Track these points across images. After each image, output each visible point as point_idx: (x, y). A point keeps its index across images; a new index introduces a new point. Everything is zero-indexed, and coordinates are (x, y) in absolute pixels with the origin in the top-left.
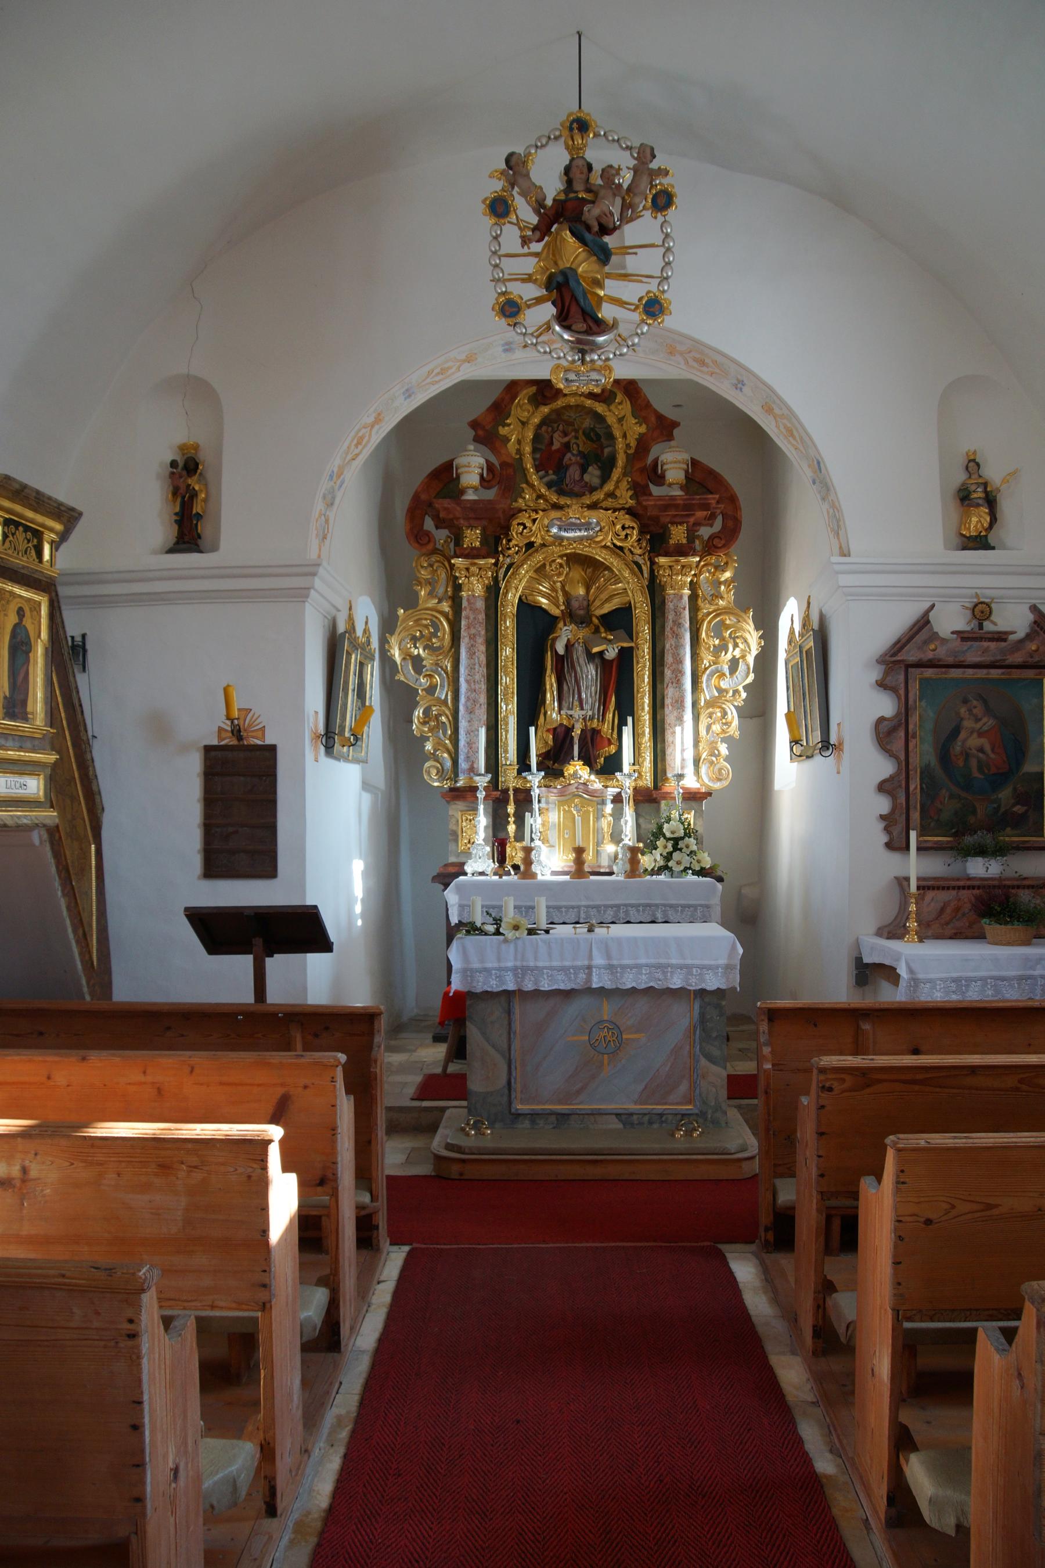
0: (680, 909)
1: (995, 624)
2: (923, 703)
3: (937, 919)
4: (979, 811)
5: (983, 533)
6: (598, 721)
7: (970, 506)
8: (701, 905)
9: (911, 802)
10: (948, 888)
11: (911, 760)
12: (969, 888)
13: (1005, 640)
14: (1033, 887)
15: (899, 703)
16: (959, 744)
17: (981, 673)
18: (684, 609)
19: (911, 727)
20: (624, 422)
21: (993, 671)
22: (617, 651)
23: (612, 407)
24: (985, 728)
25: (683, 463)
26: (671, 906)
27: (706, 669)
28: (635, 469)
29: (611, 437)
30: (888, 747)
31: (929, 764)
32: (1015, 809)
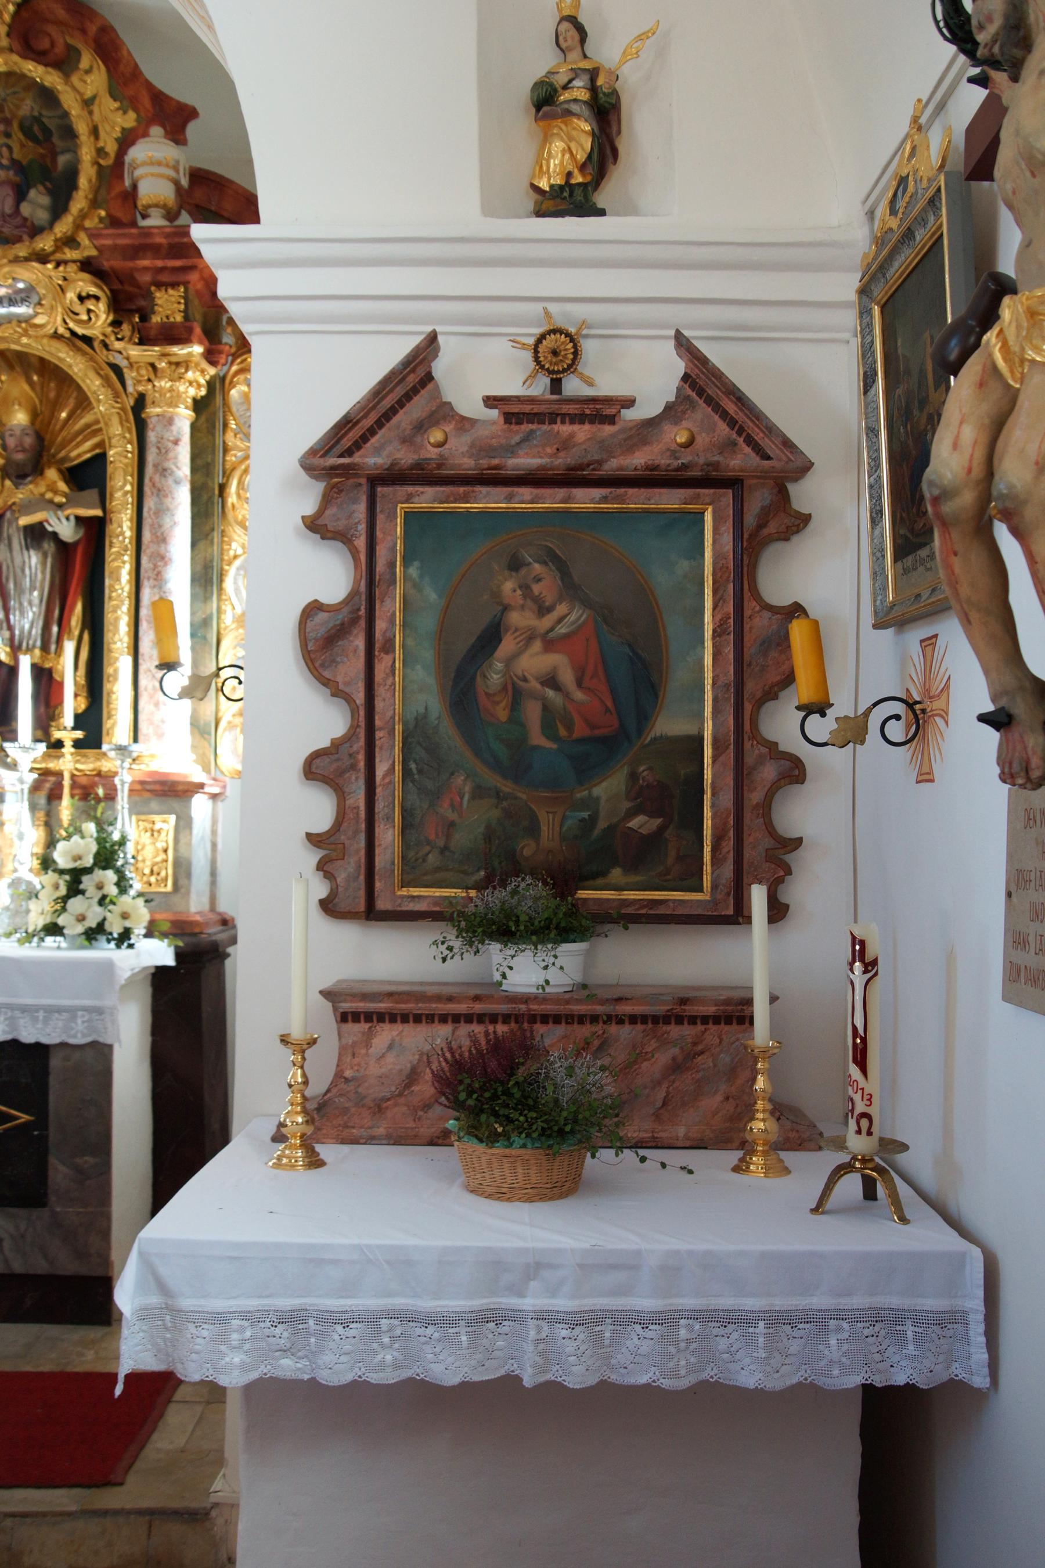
0: (41, 1015)
1: (590, 383)
2: (414, 571)
3: (401, 1095)
4: (544, 828)
5: (578, 178)
7: (552, 116)
8: (86, 1009)
9: (380, 806)
10: (430, 1018)
11: (379, 705)
12: (481, 1018)
13: (611, 420)
14: (644, 1019)
15: (356, 568)
16: (499, 666)
17: (551, 500)
18: (176, 442)
19: (380, 625)
20: (95, 108)
21: (579, 492)
23: (75, 79)
24: (562, 630)
25: (167, 166)
26: (25, 1009)
27: (236, 557)
28: (113, 195)
29: (70, 133)
30: (327, 674)
31: (425, 716)
32: (634, 823)
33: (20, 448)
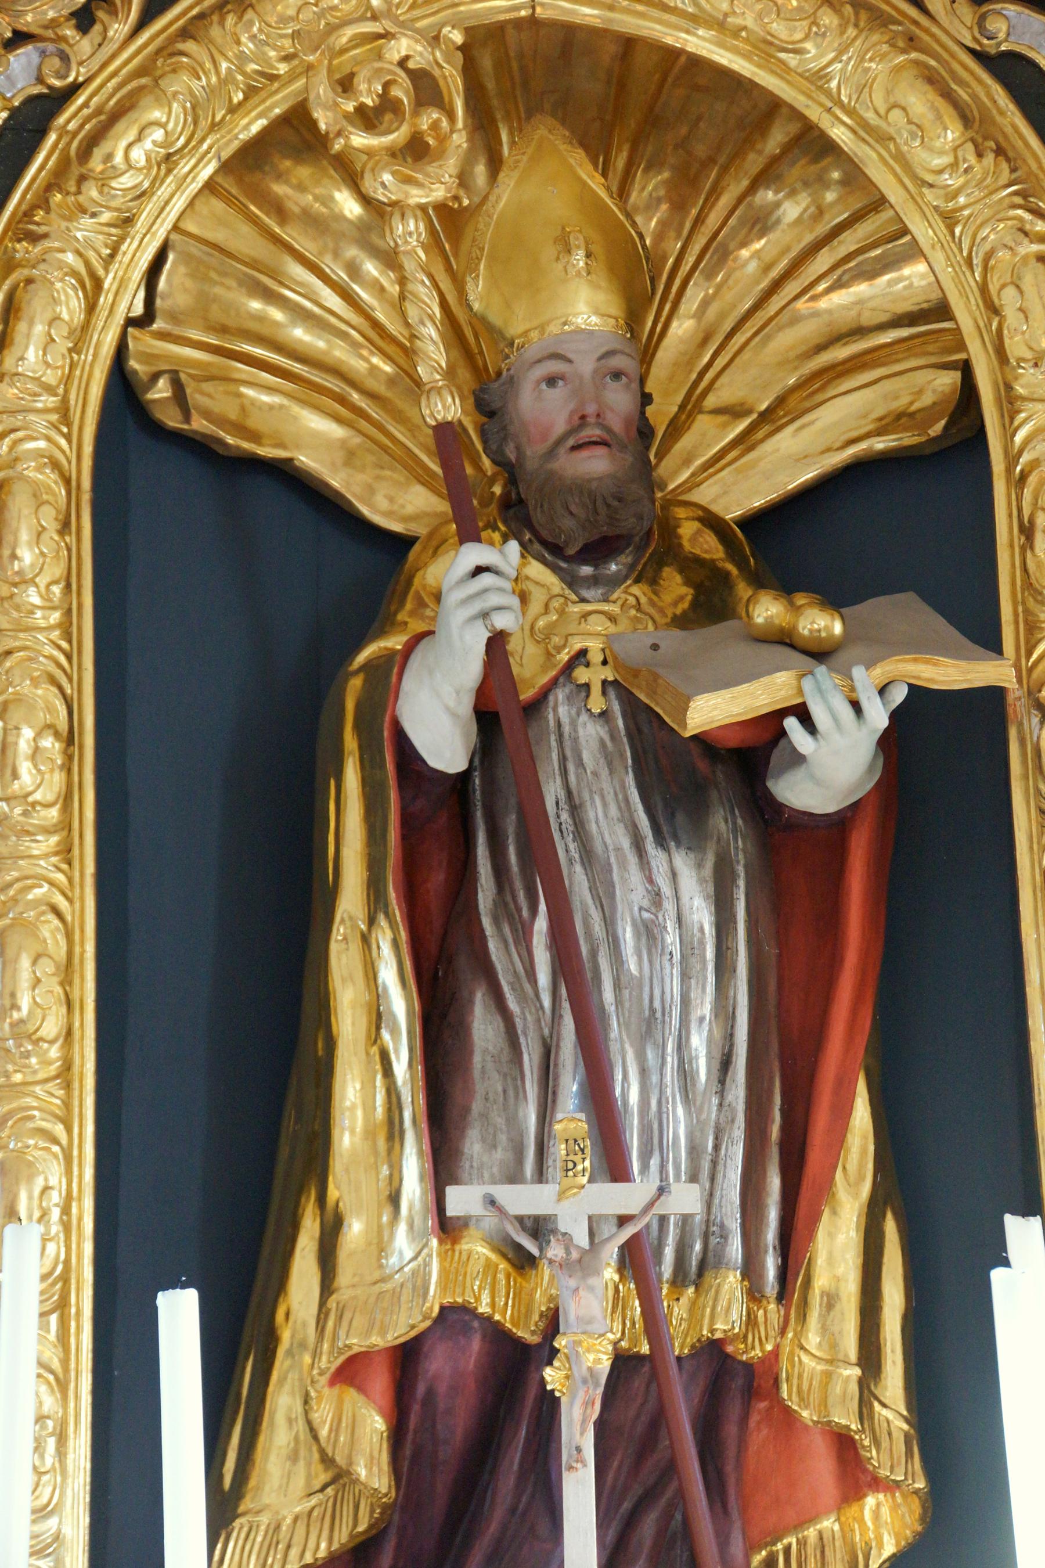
6: (754, 1294)
22: (878, 717)
33: (593, 432)
